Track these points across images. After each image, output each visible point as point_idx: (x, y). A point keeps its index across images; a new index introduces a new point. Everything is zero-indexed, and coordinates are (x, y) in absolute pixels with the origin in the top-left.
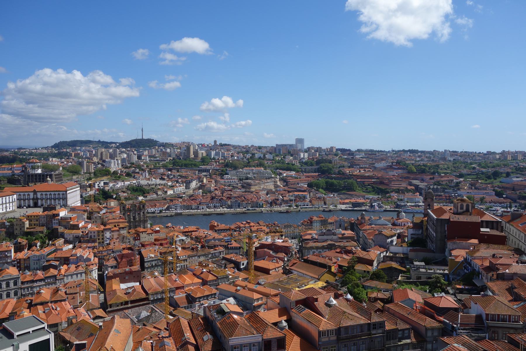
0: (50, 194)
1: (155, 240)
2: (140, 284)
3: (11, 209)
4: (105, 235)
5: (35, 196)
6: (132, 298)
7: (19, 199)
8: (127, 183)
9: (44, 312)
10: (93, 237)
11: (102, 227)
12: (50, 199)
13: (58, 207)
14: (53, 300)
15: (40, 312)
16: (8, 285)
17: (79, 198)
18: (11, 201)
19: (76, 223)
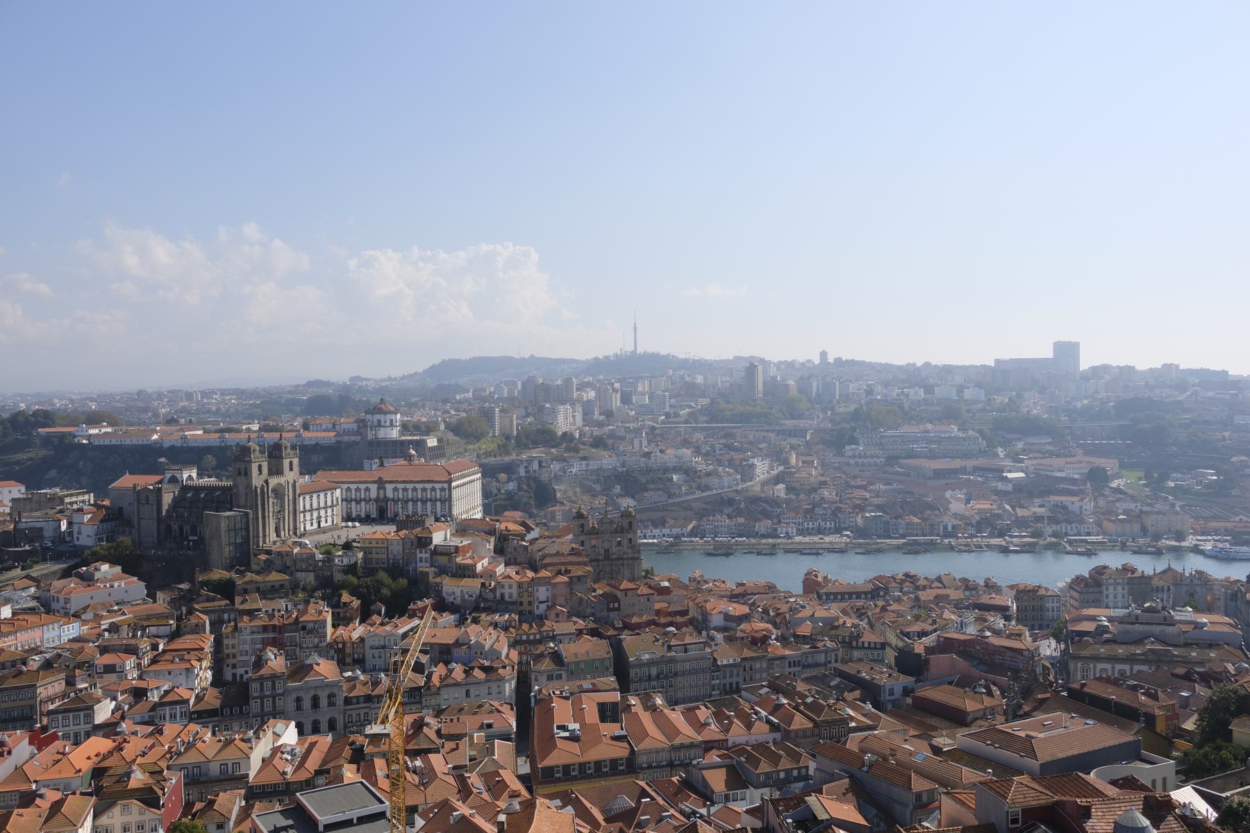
0: (415, 489)
1: (658, 612)
3: (330, 523)
4: (536, 595)
5: (382, 492)
9: (388, 776)
10: (507, 598)
11: (530, 574)
12: (415, 501)
13: (430, 521)
14: (410, 747)
15: (379, 773)
16: (315, 702)
17: (478, 499)
18: (329, 503)
19: (469, 561)
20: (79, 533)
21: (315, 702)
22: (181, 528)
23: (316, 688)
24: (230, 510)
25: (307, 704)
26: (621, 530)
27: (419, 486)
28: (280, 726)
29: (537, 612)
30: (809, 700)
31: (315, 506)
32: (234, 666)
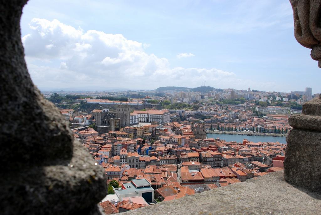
0: (155, 116)
1: (210, 147)
2: (200, 171)
3: (136, 122)
6: (195, 179)
7: (141, 118)
8: (195, 112)
10: (175, 141)
12: (155, 119)
16: (133, 160)
20: (86, 121)
21: (133, 160)
22: (106, 122)
23: (133, 158)
24: (116, 118)
25: (132, 161)
26: (201, 128)
27: (156, 115)
28: (126, 166)
29: (182, 145)
30: (245, 169)
31: (133, 118)
32: (116, 152)
